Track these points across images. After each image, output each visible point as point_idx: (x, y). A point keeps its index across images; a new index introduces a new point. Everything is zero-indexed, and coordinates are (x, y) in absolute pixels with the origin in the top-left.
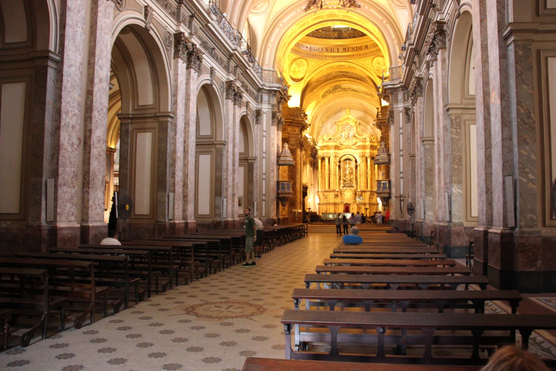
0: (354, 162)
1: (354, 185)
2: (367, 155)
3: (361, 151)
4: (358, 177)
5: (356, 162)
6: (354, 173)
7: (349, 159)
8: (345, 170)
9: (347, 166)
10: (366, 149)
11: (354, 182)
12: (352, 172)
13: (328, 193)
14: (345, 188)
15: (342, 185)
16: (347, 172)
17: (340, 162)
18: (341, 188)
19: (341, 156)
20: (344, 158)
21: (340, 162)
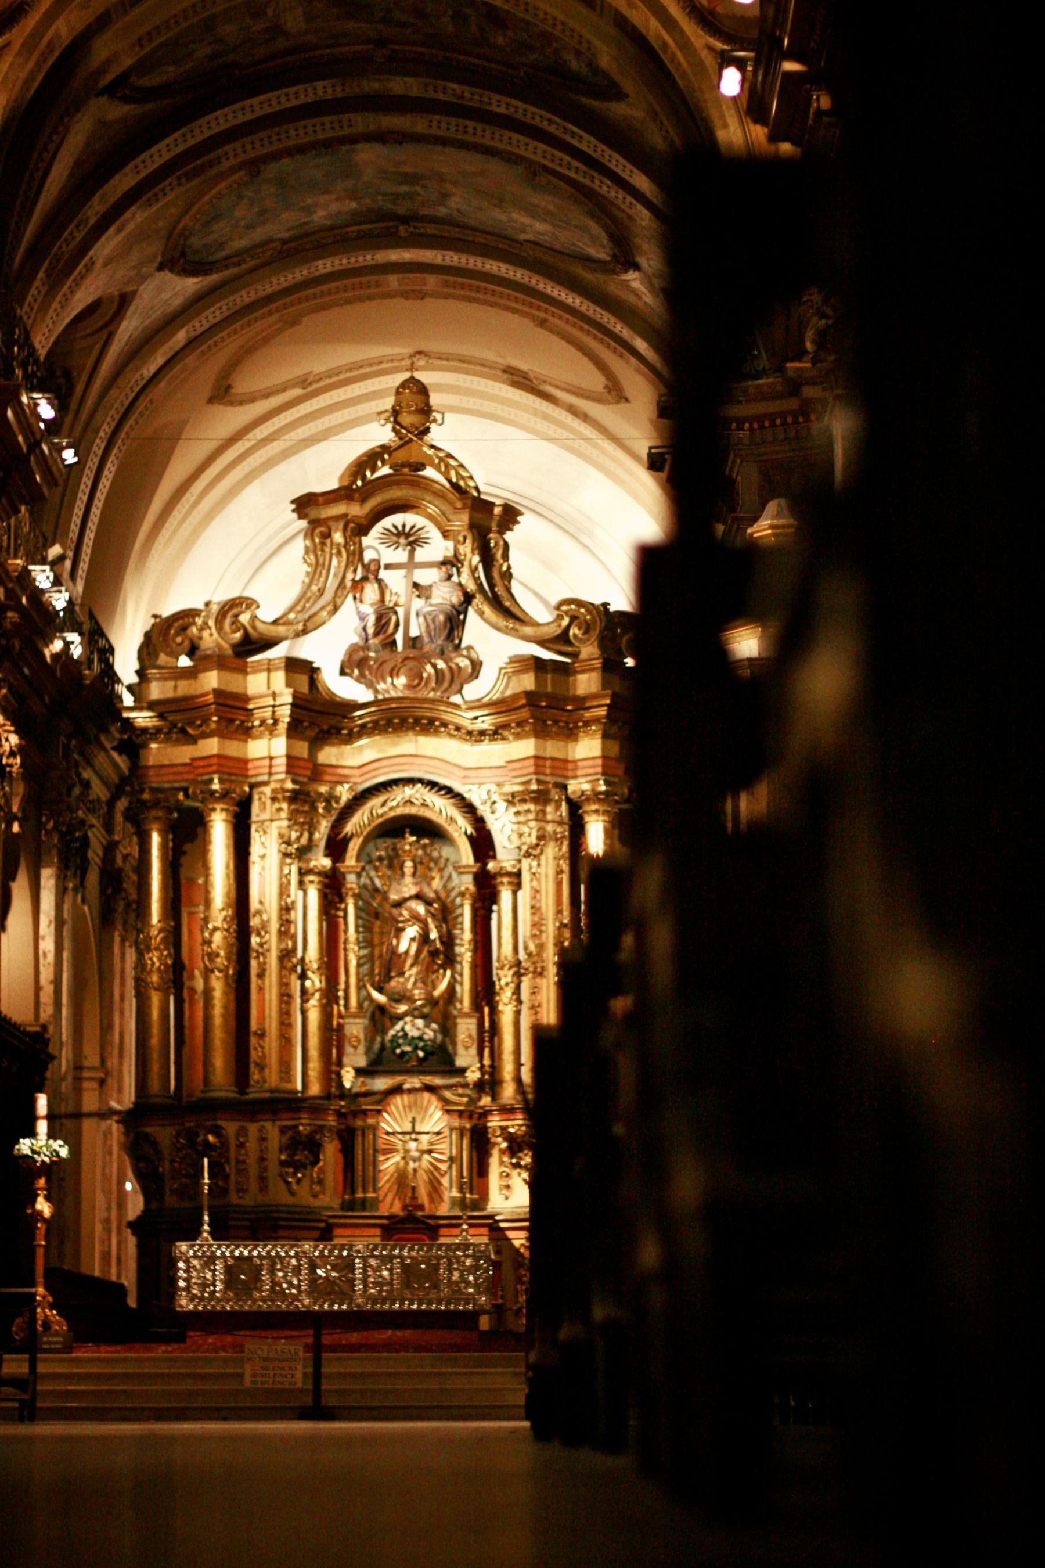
0: (466, 855)
1: (466, 1057)
2: (578, 786)
3: (525, 747)
4: (504, 978)
5: (483, 843)
6: (465, 952)
7: (429, 830)
8: (380, 919)
9: (408, 887)
10: (570, 733)
11: (466, 1028)
12: (449, 941)
13: (230, 1127)
14: (381, 1084)
15: (356, 1058)
16: (407, 941)
17: (336, 847)
18: (348, 1078)
19: (344, 793)
20: (376, 809)
21: (336, 847)
